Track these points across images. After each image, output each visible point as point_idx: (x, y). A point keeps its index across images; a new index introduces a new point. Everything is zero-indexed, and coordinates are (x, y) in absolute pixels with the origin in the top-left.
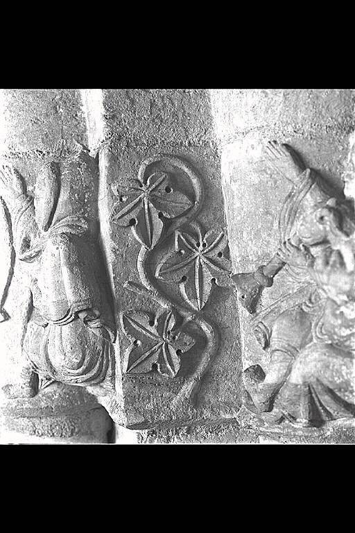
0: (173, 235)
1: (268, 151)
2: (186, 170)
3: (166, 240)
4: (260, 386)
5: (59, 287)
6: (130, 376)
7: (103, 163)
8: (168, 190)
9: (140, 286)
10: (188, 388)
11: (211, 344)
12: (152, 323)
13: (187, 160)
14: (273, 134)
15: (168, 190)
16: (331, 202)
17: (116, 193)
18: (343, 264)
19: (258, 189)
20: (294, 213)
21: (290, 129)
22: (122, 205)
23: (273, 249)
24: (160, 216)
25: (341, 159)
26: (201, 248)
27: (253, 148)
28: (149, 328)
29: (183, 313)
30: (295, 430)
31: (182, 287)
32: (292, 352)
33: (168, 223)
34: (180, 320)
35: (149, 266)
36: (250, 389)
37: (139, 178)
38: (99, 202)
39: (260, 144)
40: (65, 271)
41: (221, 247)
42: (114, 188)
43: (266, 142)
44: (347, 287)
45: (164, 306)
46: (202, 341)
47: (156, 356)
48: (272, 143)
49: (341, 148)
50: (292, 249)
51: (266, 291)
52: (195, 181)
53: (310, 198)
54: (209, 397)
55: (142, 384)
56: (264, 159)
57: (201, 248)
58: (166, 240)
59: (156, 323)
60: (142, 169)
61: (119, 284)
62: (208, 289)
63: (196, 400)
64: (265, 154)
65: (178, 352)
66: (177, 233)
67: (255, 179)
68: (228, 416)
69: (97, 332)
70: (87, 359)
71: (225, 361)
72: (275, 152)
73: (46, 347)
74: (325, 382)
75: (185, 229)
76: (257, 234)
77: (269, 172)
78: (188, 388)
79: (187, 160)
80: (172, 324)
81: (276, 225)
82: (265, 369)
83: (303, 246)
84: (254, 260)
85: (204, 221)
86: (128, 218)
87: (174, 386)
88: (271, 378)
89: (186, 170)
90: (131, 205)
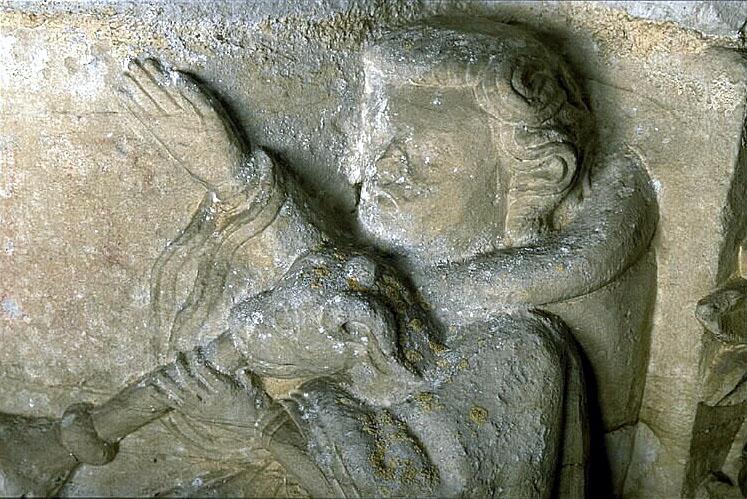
1: (132, 87)
14: (147, 39)
18: (430, 469)
25: (340, 115)
27: (72, 70)
39: (102, 64)
43: (121, 59)
48: (148, 66)
49: (341, 84)
50: (217, 387)
56: (112, 106)
64: (124, 97)
72: (157, 95)
77: (128, 148)
83: (248, 372)
84: (48, 382)
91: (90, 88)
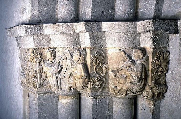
0: (100, 63)
2: (102, 52)
3: (99, 64)
4: (117, 89)
5: (81, 73)
6: (92, 88)
7: (88, 51)
8: (100, 56)
9: (94, 72)
10: (101, 90)
11: (105, 82)
12: (96, 79)
13: (102, 51)
15: (100, 56)
16: (131, 60)
17: (91, 57)
18: (134, 71)
19: (117, 57)
20: (124, 61)
21: (123, 48)
22: (93, 58)
23: (120, 67)
24: (98, 60)
26: (104, 66)
28: (95, 80)
29: (101, 77)
30: (122, 96)
31: (101, 72)
32: (123, 84)
33: (99, 61)
34: (100, 78)
35: (96, 69)
36: (115, 90)
37: (95, 54)
38: (87, 58)
40: (82, 70)
41: (107, 65)
42: (91, 56)
44: (135, 74)
45: (98, 76)
46: (103, 81)
47: (96, 84)
51: (118, 73)
52: (104, 54)
53: (127, 60)
54: (104, 91)
55: (94, 89)
57: (104, 66)
58: (99, 64)
59: (97, 79)
60: (96, 52)
61: (91, 72)
62: (105, 73)
63: (102, 92)
65: (100, 84)
66: (101, 63)
67: (117, 55)
68: (107, 94)
69: (87, 81)
70: (84, 85)
71: (107, 85)
73: (76, 83)
74: (130, 89)
75: (102, 62)
76: (117, 64)
78: (101, 90)
79: (102, 51)
80: (99, 79)
81: (120, 63)
82: (117, 86)
85: (105, 61)
86: (93, 61)
87: (99, 89)
88: (119, 88)
89: (102, 52)
90: (94, 58)
91: (117, 51)
